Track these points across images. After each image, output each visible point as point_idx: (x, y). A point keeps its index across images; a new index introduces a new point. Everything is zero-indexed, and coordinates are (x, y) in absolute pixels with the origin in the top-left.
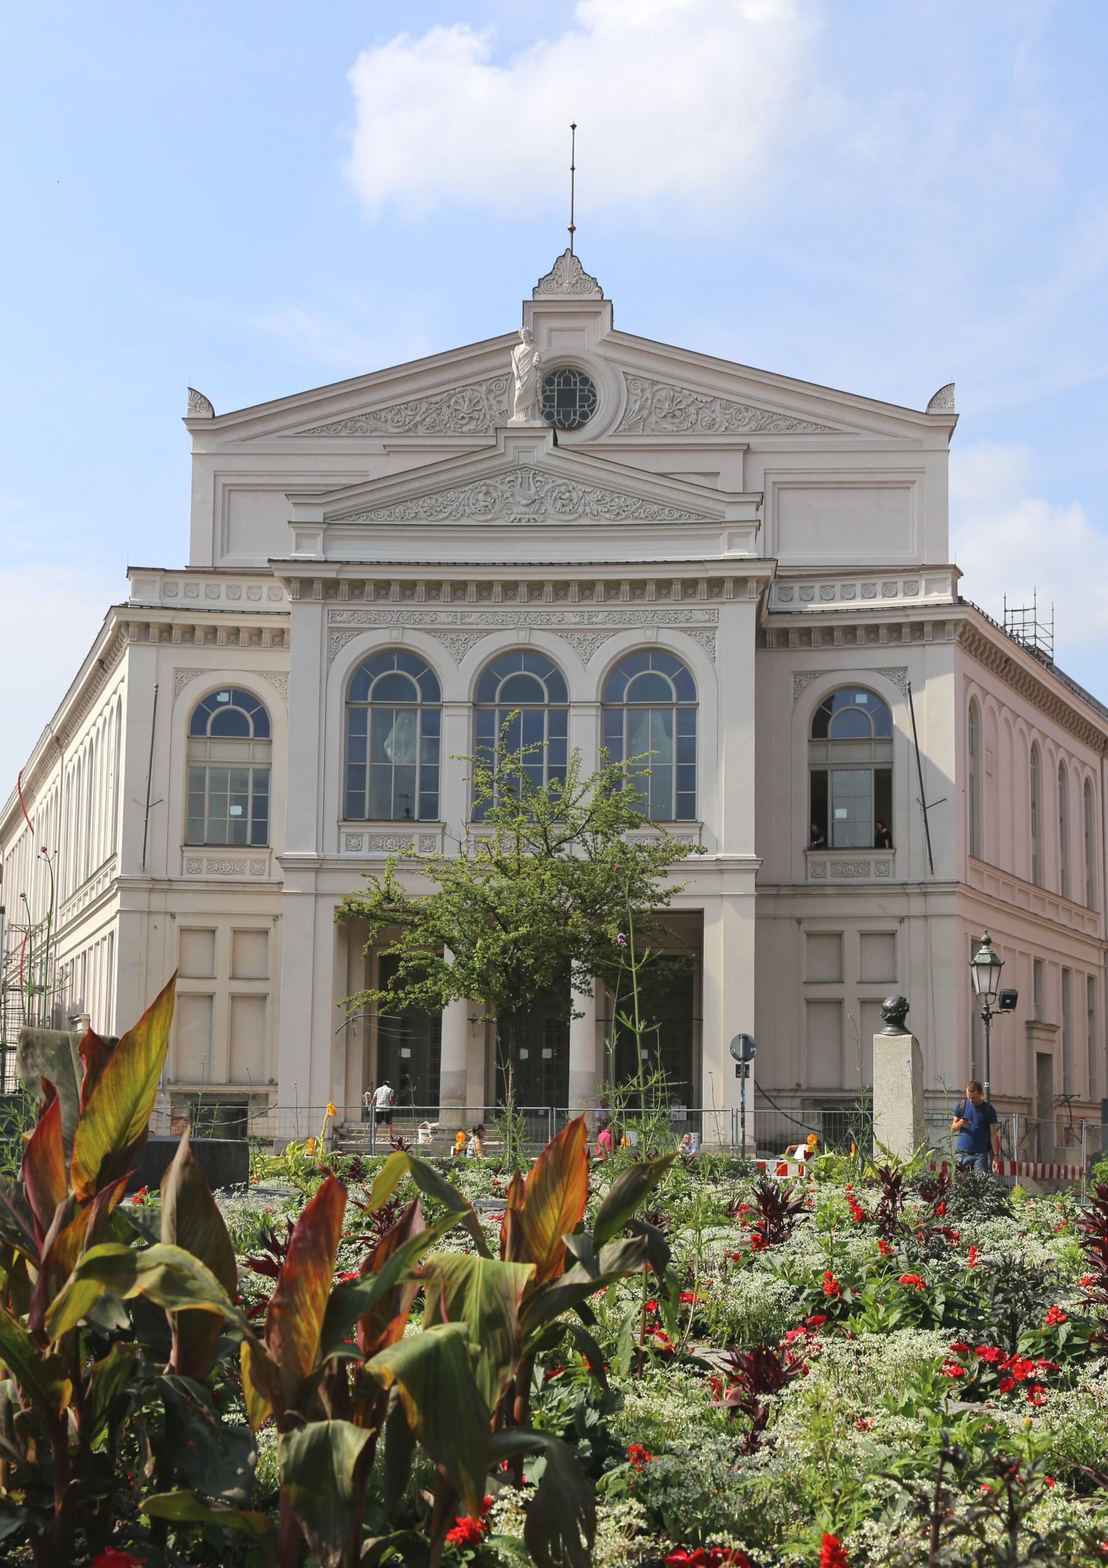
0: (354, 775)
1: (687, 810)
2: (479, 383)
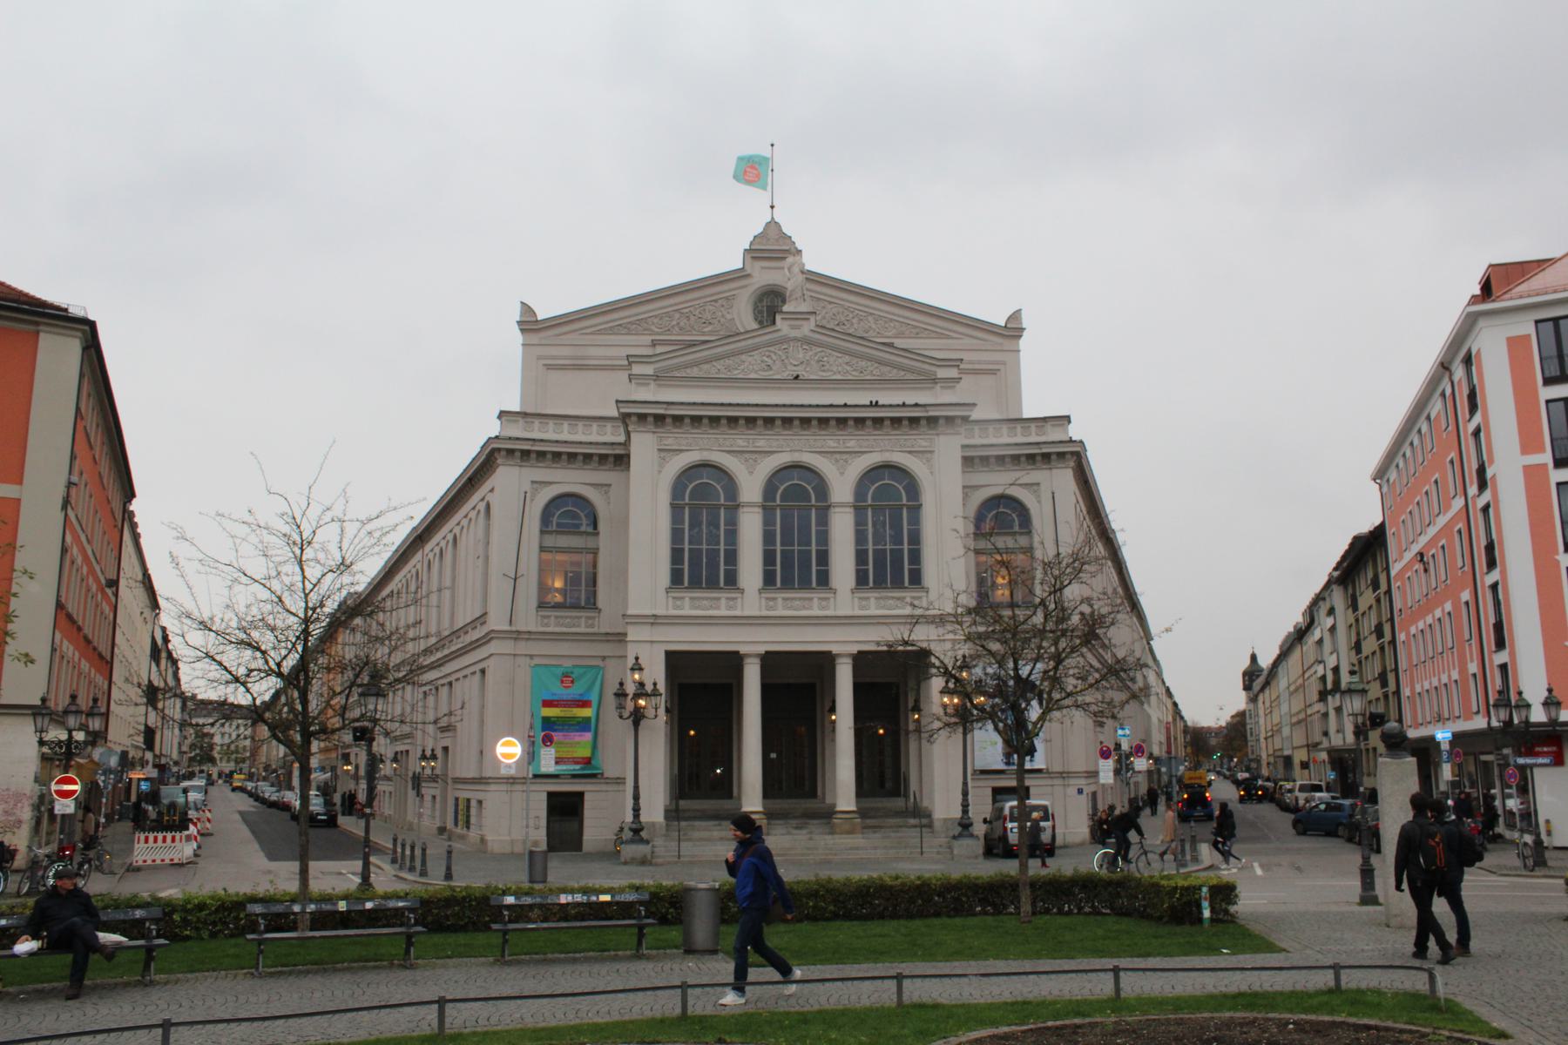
0: (676, 555)
1: (916, 579)
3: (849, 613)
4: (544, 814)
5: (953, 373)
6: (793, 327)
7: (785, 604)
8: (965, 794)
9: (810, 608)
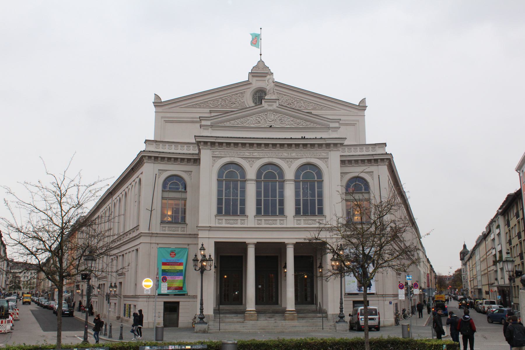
0: (220, 201)
1: (321, 212)
2: (237, 94)
3: (292, 226)
4: (162, 311)
5: (337, 125)
6: (269, 105)
7: (264, 222)
8: (341, 303)
9: (276, 224)
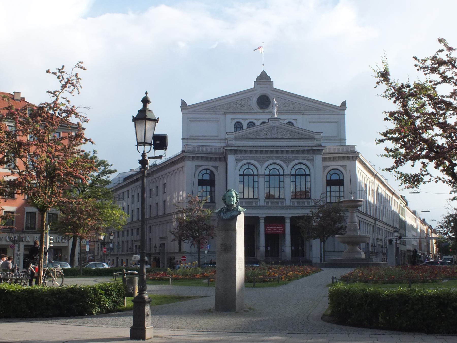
6: (273, 123)
